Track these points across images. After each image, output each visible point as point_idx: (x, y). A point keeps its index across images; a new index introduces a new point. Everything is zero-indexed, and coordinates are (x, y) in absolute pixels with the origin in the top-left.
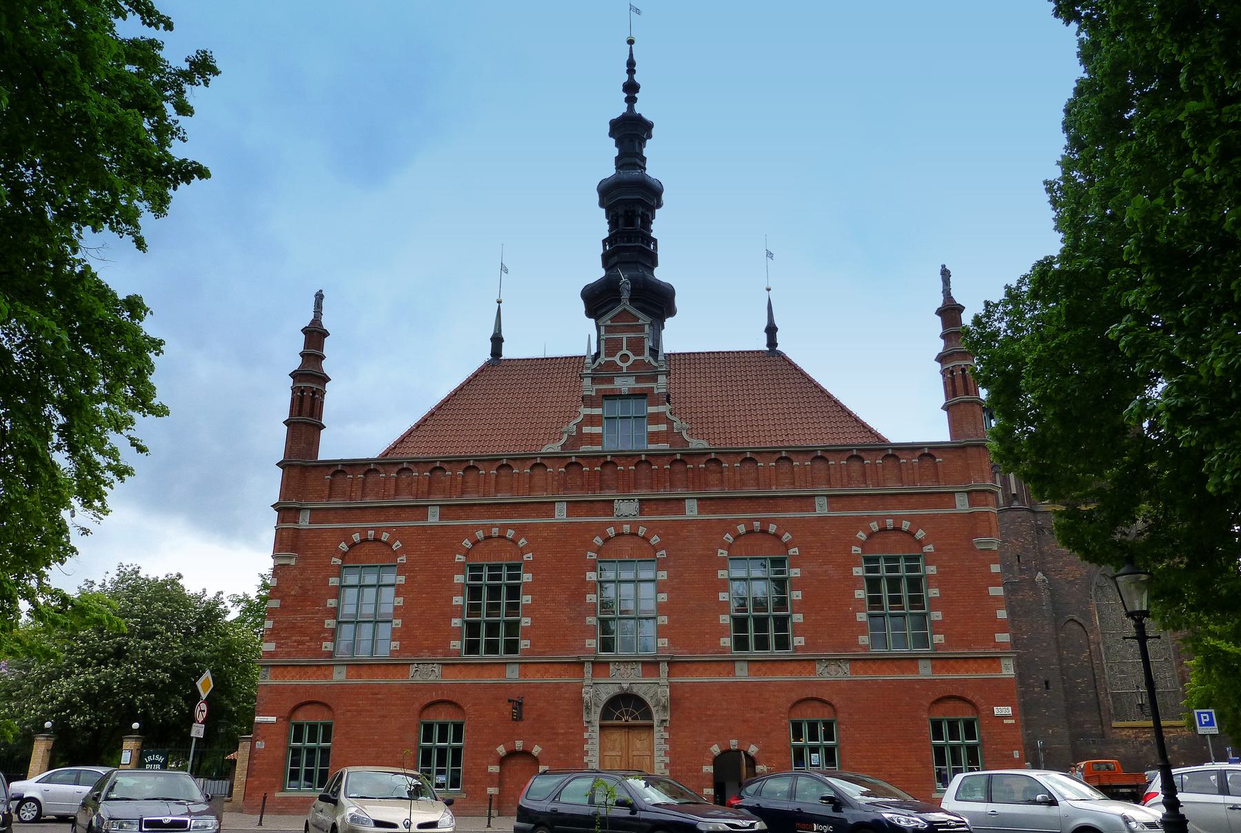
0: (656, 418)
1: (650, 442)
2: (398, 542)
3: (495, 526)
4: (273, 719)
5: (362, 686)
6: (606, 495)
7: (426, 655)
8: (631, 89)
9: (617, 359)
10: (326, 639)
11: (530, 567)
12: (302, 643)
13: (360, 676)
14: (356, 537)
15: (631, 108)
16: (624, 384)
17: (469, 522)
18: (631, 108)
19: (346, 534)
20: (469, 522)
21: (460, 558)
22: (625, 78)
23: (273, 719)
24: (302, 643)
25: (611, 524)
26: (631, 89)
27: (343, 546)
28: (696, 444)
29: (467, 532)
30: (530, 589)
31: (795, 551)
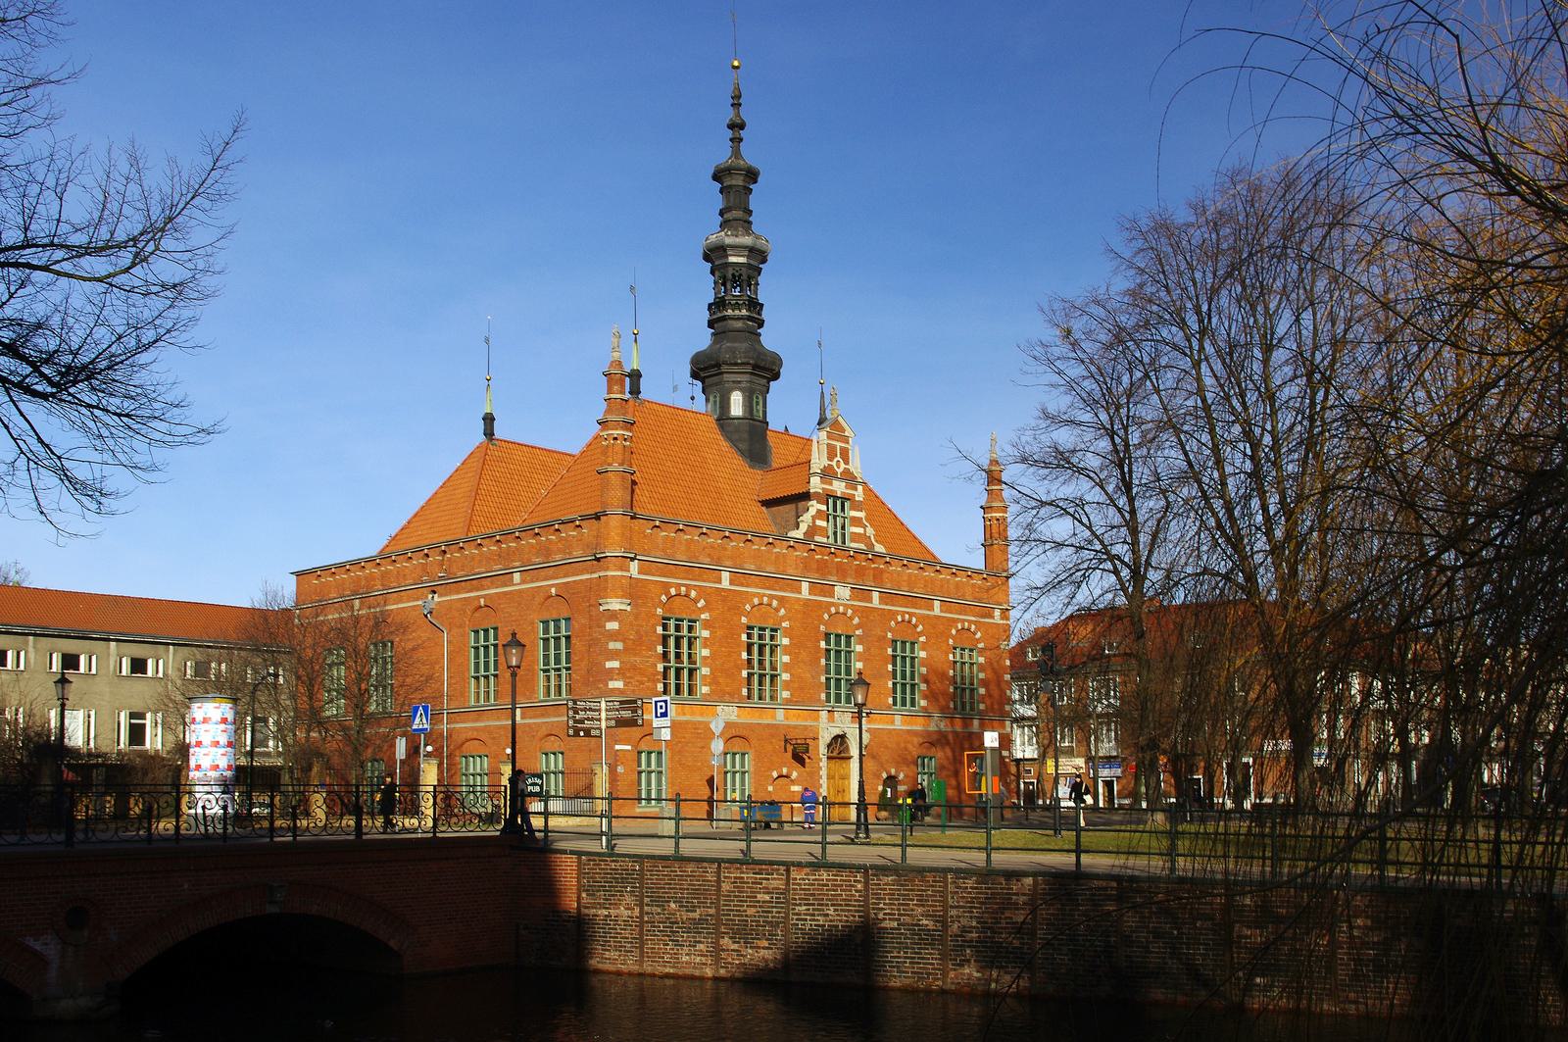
0: (856, 521)
1: (852, 541)
2: (702, 601)
3: (764, 595)
4: (629, 748)
5: (687, 722)
6: (831, 580)
7: (727, 698)
8: (737, 126)
9: (834, 463)
10: (658, 681)
11: (787, 633)
12: (642, 683)
13: (684, 714)
14: (673, 591)
15: (736, 153)
16: (839, 487)
17: (749, 590)
18: (736, 153)
19: (666, 586)
20: (749, 590)
21: (744, 620)
22: (729, 114)
23: (629, 748)
24: (642, 683)
25: (833, 604)
26: (737, 126)
27: (664, 598)
28: (879, 548)
29: (748, 597)
30: (787, 650)
31: (922, 639)
